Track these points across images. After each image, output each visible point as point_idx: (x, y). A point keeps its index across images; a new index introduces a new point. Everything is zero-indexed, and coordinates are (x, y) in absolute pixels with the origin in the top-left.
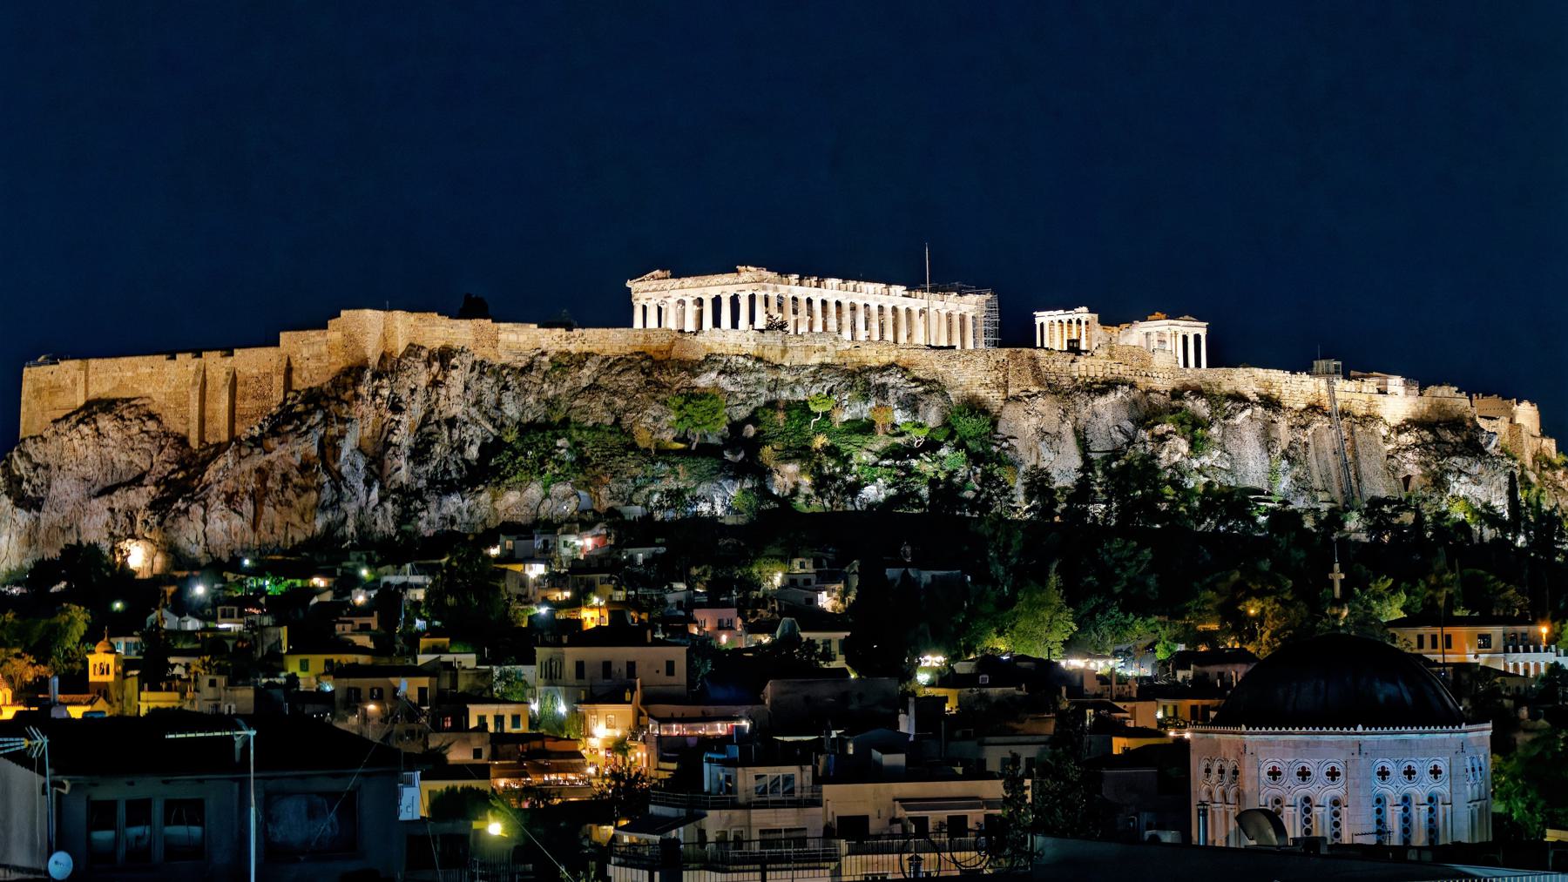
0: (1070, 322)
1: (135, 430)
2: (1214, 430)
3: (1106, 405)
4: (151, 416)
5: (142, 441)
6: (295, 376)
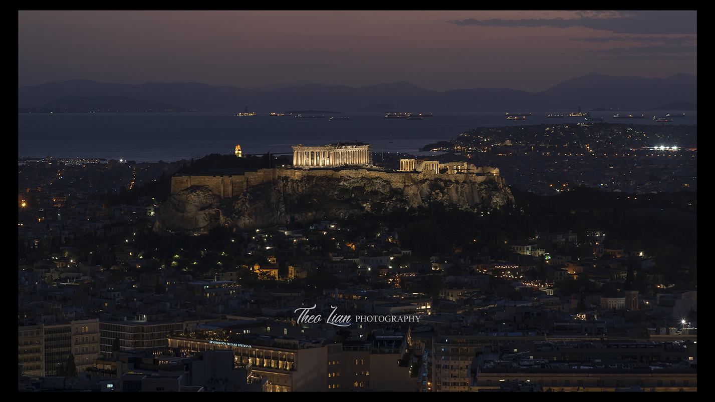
0: (410, 162)
1: (207, 194)
2: (446, 190)
3: (425, 186)
4: (210, 191)
5: (209, 197)
6: (249, 183)
